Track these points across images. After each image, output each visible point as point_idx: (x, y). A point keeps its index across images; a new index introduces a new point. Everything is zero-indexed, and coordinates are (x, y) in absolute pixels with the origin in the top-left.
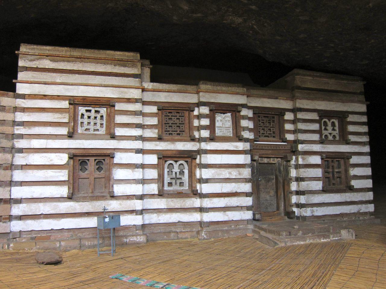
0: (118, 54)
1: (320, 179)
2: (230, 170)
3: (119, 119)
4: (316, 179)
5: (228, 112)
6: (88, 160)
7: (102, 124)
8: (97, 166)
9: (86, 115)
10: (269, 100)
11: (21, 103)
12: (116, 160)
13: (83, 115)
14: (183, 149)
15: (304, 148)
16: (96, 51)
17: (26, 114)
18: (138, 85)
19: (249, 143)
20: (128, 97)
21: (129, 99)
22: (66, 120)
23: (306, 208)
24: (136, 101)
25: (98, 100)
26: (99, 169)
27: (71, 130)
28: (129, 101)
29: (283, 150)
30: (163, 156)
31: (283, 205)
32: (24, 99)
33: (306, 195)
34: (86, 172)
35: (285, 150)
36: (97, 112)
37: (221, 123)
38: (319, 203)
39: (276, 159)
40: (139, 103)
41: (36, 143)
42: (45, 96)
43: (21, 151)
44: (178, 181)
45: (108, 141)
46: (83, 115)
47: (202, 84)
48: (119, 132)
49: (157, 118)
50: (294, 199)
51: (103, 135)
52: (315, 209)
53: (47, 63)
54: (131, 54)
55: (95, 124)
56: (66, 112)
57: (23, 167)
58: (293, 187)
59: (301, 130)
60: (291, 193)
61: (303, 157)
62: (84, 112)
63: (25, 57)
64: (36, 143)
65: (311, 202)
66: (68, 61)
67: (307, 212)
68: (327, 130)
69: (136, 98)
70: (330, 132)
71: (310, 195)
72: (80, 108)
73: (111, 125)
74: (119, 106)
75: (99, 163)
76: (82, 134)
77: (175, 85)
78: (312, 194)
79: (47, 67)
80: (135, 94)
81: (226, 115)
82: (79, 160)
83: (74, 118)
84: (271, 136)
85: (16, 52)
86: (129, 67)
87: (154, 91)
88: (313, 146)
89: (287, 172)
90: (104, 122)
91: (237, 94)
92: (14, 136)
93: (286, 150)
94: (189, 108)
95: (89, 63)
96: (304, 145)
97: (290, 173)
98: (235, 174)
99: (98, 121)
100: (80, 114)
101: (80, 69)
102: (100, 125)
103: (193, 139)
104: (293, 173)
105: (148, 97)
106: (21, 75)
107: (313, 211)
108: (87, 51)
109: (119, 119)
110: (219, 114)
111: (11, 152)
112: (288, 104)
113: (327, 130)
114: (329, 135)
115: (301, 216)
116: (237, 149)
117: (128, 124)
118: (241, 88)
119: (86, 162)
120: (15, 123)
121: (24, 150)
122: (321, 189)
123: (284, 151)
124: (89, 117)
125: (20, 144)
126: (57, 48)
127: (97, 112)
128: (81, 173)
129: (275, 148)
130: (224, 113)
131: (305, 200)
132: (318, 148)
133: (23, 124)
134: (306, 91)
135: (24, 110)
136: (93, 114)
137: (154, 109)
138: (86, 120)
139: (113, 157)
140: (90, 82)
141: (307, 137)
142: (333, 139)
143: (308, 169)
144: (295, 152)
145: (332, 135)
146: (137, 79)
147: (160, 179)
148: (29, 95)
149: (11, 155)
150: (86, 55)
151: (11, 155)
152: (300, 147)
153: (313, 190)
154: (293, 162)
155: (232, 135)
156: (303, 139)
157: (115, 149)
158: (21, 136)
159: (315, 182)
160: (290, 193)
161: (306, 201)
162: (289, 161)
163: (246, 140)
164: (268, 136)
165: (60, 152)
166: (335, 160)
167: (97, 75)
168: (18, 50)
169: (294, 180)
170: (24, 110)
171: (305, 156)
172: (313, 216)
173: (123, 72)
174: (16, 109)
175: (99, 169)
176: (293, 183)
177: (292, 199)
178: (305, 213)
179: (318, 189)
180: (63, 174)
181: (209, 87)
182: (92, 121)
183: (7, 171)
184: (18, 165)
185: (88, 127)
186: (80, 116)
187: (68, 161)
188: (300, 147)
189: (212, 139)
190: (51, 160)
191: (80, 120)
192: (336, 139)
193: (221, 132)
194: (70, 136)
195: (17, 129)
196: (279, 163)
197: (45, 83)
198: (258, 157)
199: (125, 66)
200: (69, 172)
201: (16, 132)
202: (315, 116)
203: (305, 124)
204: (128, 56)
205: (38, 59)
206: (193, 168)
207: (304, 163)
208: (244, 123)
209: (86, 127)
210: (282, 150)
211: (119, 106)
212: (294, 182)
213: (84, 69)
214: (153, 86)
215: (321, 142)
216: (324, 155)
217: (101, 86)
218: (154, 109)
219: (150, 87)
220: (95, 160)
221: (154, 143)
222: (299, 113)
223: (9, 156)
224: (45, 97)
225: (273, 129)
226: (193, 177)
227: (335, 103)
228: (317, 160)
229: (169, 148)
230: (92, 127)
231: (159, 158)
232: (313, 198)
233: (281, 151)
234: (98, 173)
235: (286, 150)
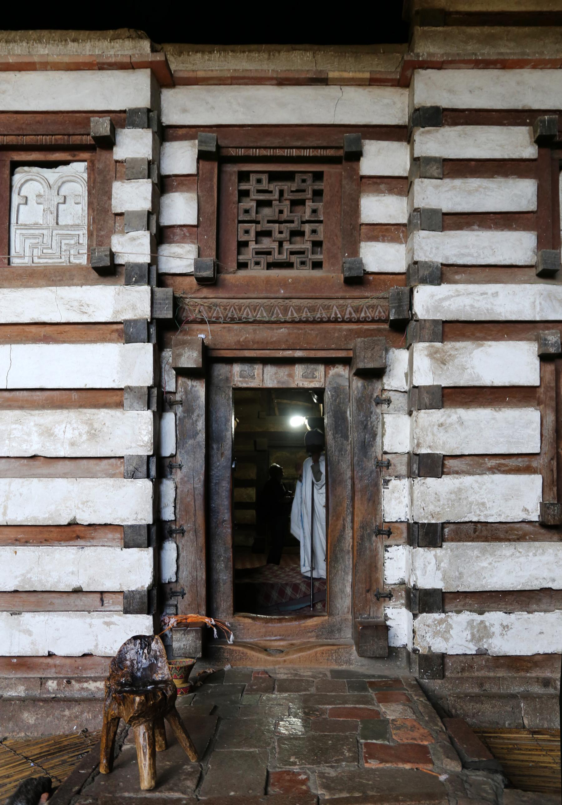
1: (534, 464)
4: (512, 462)
15: (446, 304)
23: (443, 615)
29: (350, 321)
31: (348, 590)
33: (445, 545)
35: (358, 321)
38: (519, 588)
39: (321, 368)
58: (393, 502)
59: (434, 212)
78: (486, 540)
88: (496, 294)
93: (365, 321)
96: (444, 289)
97: (383, 435)
112: (386, 101)
115: (415, 651)
122: (535, 516)
123: (354, 326)
129: (306, 314)
131: (440, 575)
141: (467, 247)
143: (461, 412)
153: (490, 520)
156: (440, 260)
159: (499, 478)
160: (379, 532)
161: (444, 579)
164: (289, 265)
169: (403, 469)
171: (449, 345)
172: (481, 654)
176: (394, 483)
177: (388, 563)
178: (439, 639)
179: (516, 515)
196: (337, 390)
203: (458, 182)
207: (445, 383)
210: (343, 321)
212: (398, 477)
222: (428, 132)
232: (485, 564)
233: (338, 326)
235: (365, 321)
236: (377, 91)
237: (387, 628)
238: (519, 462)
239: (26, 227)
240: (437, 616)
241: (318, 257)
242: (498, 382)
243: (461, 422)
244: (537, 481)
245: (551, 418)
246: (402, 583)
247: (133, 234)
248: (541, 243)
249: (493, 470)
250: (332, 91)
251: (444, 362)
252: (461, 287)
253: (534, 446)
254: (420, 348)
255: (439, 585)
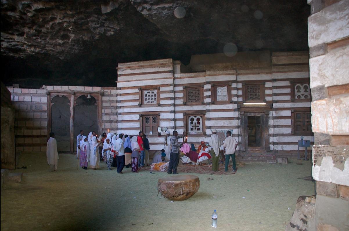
0: (161, 61)
2: (224, 121)
3: (162, 96)
5: (224, 86)
6: (149, 117)
7: (155, 99)
8: (154, 120)
9: (148, 94)
10: (254, 76)
11: (119, 92)
12: (161, 117)
13: (146, 95)
14: (197, 109)
16: (150, 61)
17: (122, 97)
18: (172, 76)
19: (236, 105)
20: (166, 84)
21: (167, 84)
22: (138, 98)
24: (170, 85)
25: (152, 87)
26: (155, 122)
27: (141, 103)
28: (167, 85)
30: (187, 114)
32: (121, 89)
34: (149, 123)
36: (152, 92)
37: (221, 93)
40: (172, 86)
41: (126, 110)
42: (129, 87)
43: (121, 114)
44: (197, 128)
45: (157, 107)
46: (146, 95)
47: (207, 71)
48: (162, 102)
49: (183, 93)
50: (272, 139)
51: (156, 104)
52: (284, 146)
53: (129, 71)
54: (167, 60)
55: (152, 99)
56: (138, 94)
57: (121, 121)
60: (270, 135)
61: (276, 112)
62: (147, 93)
63: (120, 70)
64: (126, 110)
65: (281, 142)
66: (138, 69)
67: (279, 148)
68: (300, 92)
69: (170, 83)
70: (302, 93)
71: (281, 137)
72: (145, 91)
73: (159, 99)
74: (162, 89)
75: (154, 119)
76: (146, 104)
77: (192, 74)
79: (129, 73)
80: (170, 81)
81: (223, 88)
82: (145, 117)
83: (142, 97)
84: (257, 99)
85: (116, 68)
86: (166, 67)
87: (181, 78)
89: (267, 122)
90: (156, 98)
91: (229, 74)
92: (117, 108)
94: (201, 85)
95: (147, 69)
96: (277, 104)
98: (227, 123)
99: (153, 97)
100: (145, 94)
101: (143, 72)
102: (154, 100)
103: (204, 104)
104: (271, 122)
105: (177, 82)
106: (119, 79)
107: (283, 148)
108: (146, 62)
109: (162, 96)
110: (220, 88)
111: (117, 115)
113: (300, 92)
114: (301, 95)
116: (229, 109)
117: (167, 98)
118: (232, 71)
119: (149, 118)
120: (117, 102)
121: (122, 114)
122: (290, 133)
124: (149, 96)
125: (120, 111)
126: (133, 63)
127: (152, 92)
128: (146, 124)
130: (223, 87)
132: (289, 105)
133: (121, 101)
134: (281, 67)
135: (121, 95)
136: (151, 94)
137: (181, 88)
138: (148, 97)
139: (160, 116)
140: (148, 78)
142: (305, 98)
143: (280, 120)
144: (272, 108)
145: (304, 95)
146: (171, 73)
147: (186, 126)
148: (122, 88)
149: (117, 116)
150: (146, 64)
151: (117, 116)
152: (274, 105)
154: (270, 115)
155: (227, 100)
156: (276, 100)
157: (160, 111)
158: (120, 107)
159: (285, 128)
162: (268, 114)
163: (235, 103)
165: (136, 114)
166: (306, 113)
167: (151, 74)
168: (117, 66)
170: (121, 95)
171: (278, 111)
172: (283, 150)
173: (163, 70)
174: (117, 95)
175: (155, 122)
176: (271, 128)
180: (137, 124)
181: (212, 72)
182: (150, 98)
183: (115, 123)
184: (119, 121)
185: (149, 101)
186: (145, 96)
187: (140, 118)
188: (274, 105)
189: (214, 102)
190: (132, 118)
191: (145, 97)
192: (308, 98)
193: (220, 98)
194: (140, 105)
195: (118, 104)
197: (128, 81)
198: (243, 113)
199: (164, 67)
200: (140, 123)
201: (118, 105)
202: (287, 83)
203: (279, 89)
204: (166, 61)
205: (125, 70)
206: (204, 120)
208: (234, 92)
209: (148, 101)
211: (162, 89)
212: (271, 128)
213: (145, 72)
214: (180, 75)
215: (293, 100)
216: (293, 110)
217: (152, 79)
218: (181, 88)
219: (179, 77)
220: (152, 117)
221: (181, 107)
223: (116, 117)
224: (129, 88)
225: (259, 94)
226: (204, 125)
227: (305, 72)
228: (288, 113)
229: (190, 110)
230: (150, 101)
231: (184, 115)
234: (154, 123)
236: (267, 75)
237: (270, 147)
238: (289, 126)
239: (219, 95)
240: (276, 145)
241: (259, 98)
242: (285, 116)
243: (280, 121)
244: (291, 129)
245: (293, 120)
246: (272, 142)
247: (234, 97)
248: (291, 97)
249: (285, 127)
250: (261, 75)
251: (277, 113)
252: (279, 103)
253: (290, 124)
254: (274, 111)
255: (277, 142)
